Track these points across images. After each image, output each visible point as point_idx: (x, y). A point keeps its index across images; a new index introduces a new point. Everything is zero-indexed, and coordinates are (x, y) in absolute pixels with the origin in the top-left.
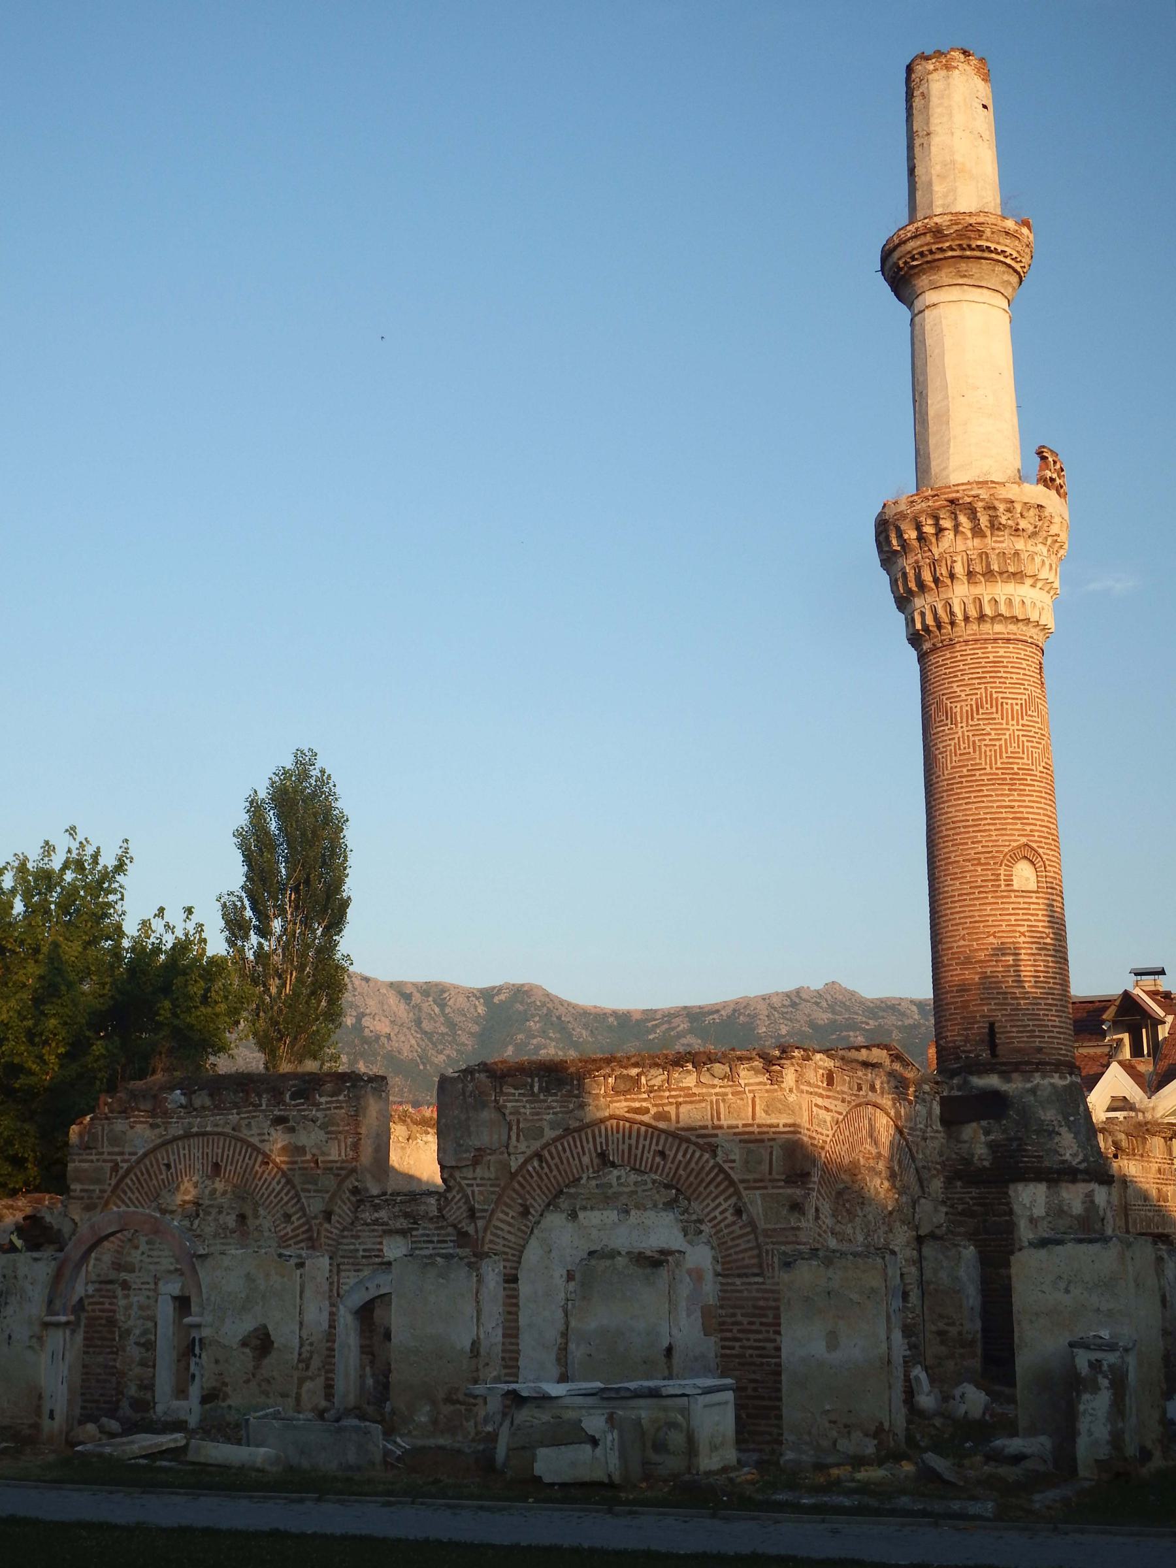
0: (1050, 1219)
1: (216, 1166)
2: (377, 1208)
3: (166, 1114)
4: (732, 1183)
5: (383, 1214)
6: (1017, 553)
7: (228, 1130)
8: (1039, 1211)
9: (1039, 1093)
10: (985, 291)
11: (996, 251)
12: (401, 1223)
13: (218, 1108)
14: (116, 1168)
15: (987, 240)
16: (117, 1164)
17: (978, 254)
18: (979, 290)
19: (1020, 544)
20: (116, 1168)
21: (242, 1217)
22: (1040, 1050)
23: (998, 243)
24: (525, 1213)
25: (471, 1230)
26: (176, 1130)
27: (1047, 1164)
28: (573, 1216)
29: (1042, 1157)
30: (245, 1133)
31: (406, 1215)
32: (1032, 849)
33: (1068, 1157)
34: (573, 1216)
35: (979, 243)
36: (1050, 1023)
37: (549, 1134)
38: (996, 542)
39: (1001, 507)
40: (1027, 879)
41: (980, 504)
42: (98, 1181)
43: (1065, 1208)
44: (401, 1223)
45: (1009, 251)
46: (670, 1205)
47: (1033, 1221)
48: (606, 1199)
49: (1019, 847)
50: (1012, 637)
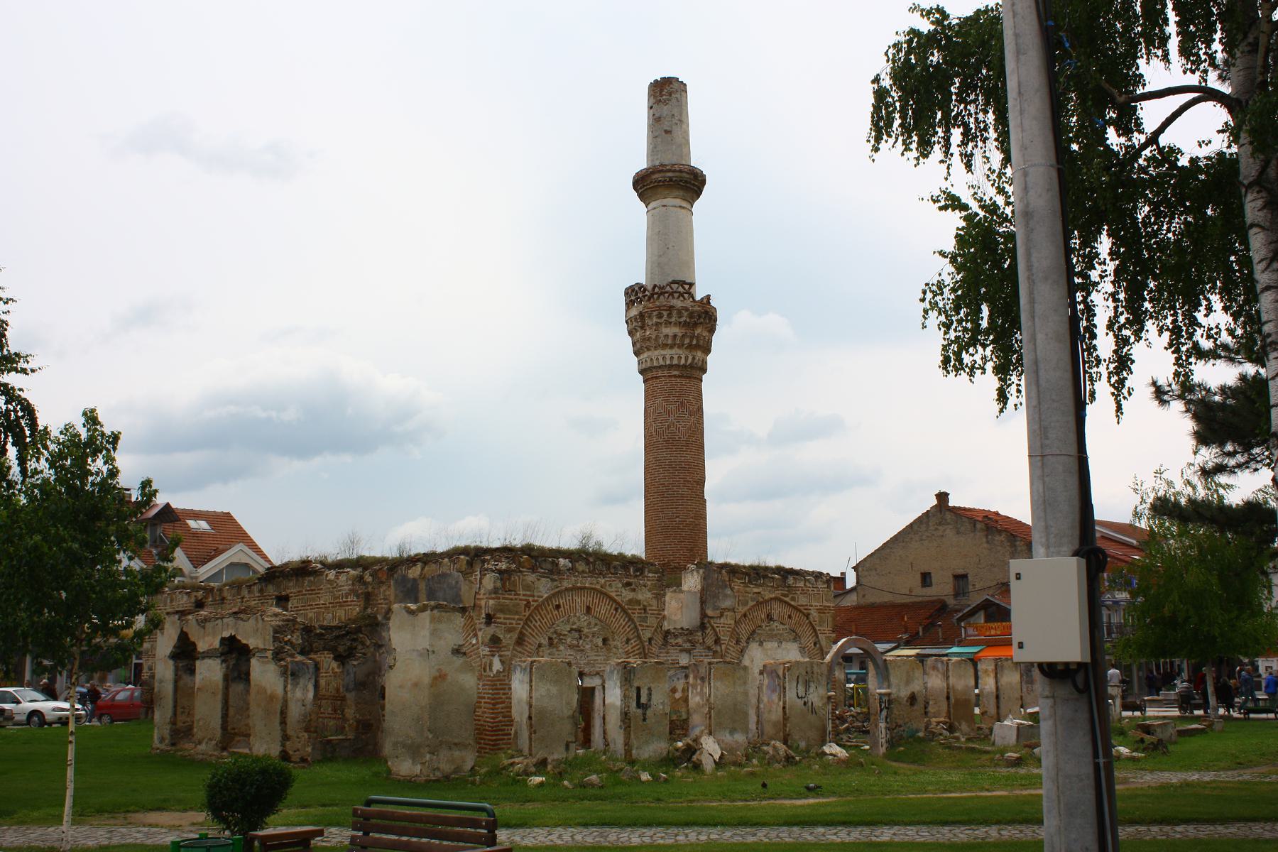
1: (588, 608)
2: (676, 636)
3: (559, 572)
4: (815, 630)
5: (680, 640)
7: (598, 587)
12: (687, 646)
13: (592, 573)
14: (528, 605)
16: (529, 602)
20: (528, 605)
21: (605, 640)
24: (738, 642)
25: (718, 648)
26: (566, 584)
28: (761, 644)
30: (607, 589)
31: (690, 641)
34: (761, 644)
37: (751, 603)
42: (517, 613)
44: (687, 646)
46: (795, 640)
48: (772, 637)
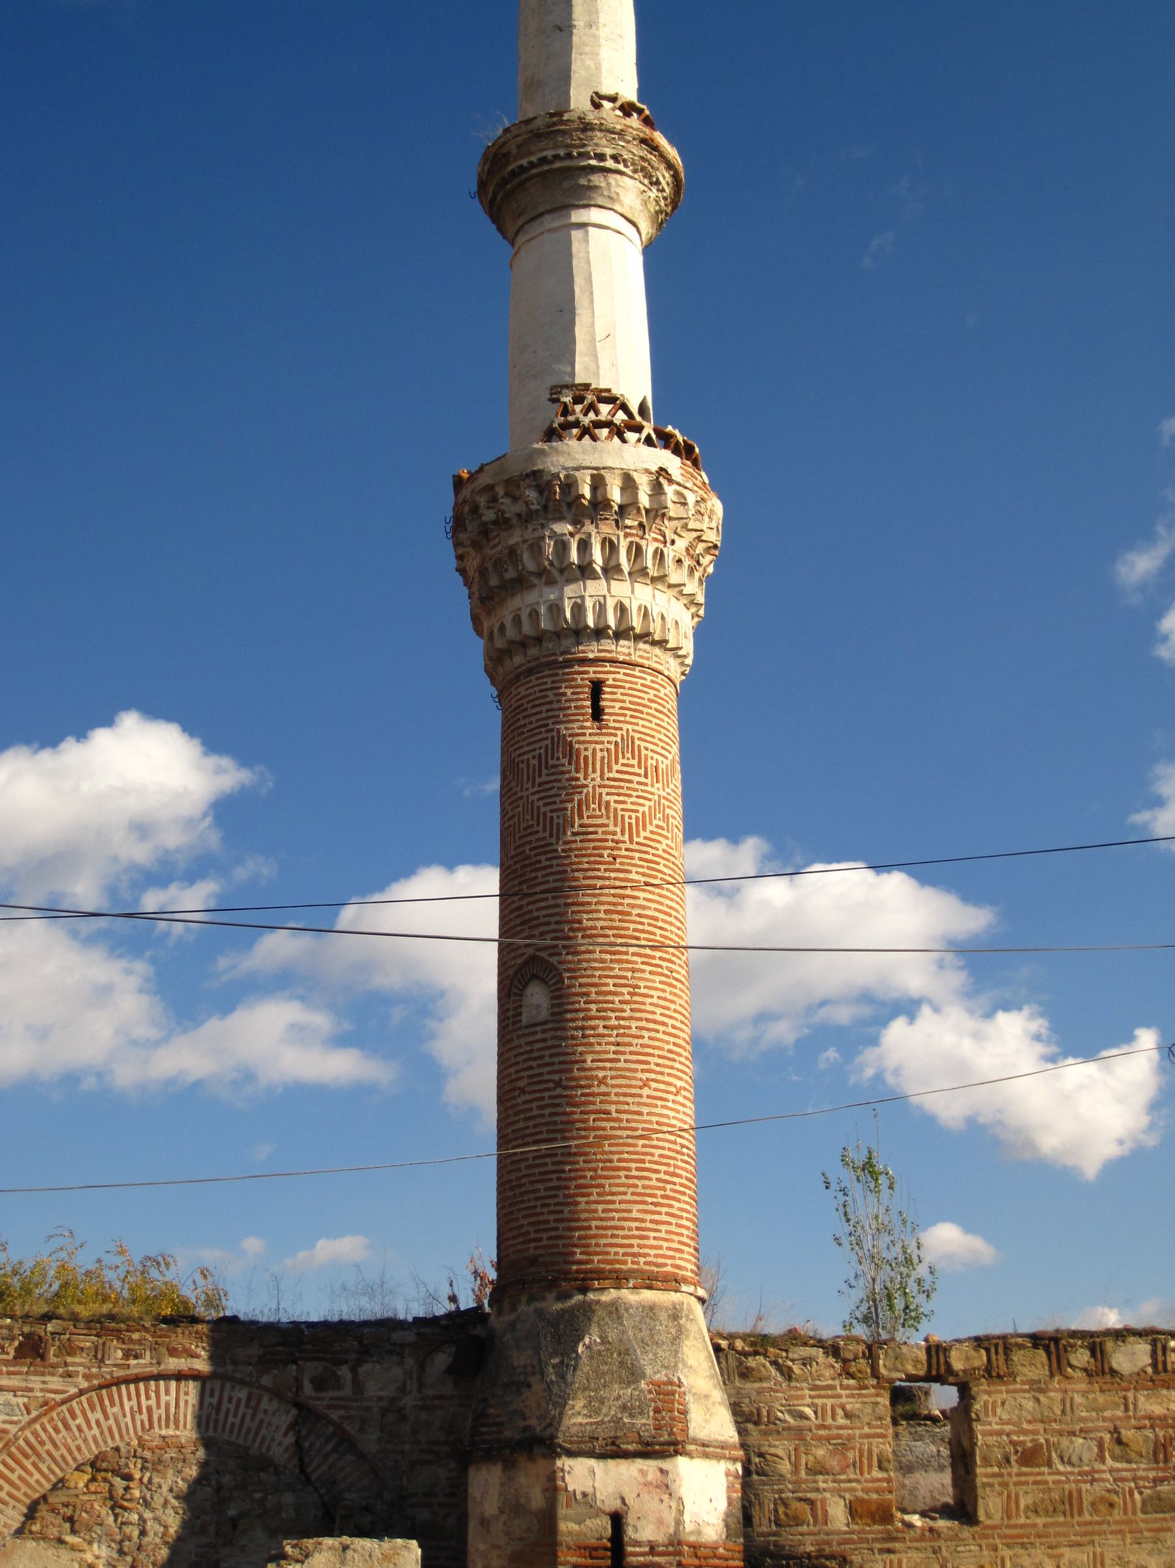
0: (504, 1518)
6: (513, 552)
8: (491, 1507)
9: (519, 1326)
10: (547, 217)
11: (532, 165)
15: (516, 159)
17: (515, 182)
18: (539, 221)
19: (515, 538)
22: (533, 1261)
23: (531, 154)
27: (508, 1434)
29: (502, 1424)
32: (542, 959)
33: (533, 1422)
35: (510, 168)
36: (552, 1217)
38: (492, 548)
39: (482, 500)
40: (538, 1006)
41: (467, 508)
43: (523, 1500)
45: (549, 153)
47: (485, 1523)
49: (526, 963)
50: (533, 664)
